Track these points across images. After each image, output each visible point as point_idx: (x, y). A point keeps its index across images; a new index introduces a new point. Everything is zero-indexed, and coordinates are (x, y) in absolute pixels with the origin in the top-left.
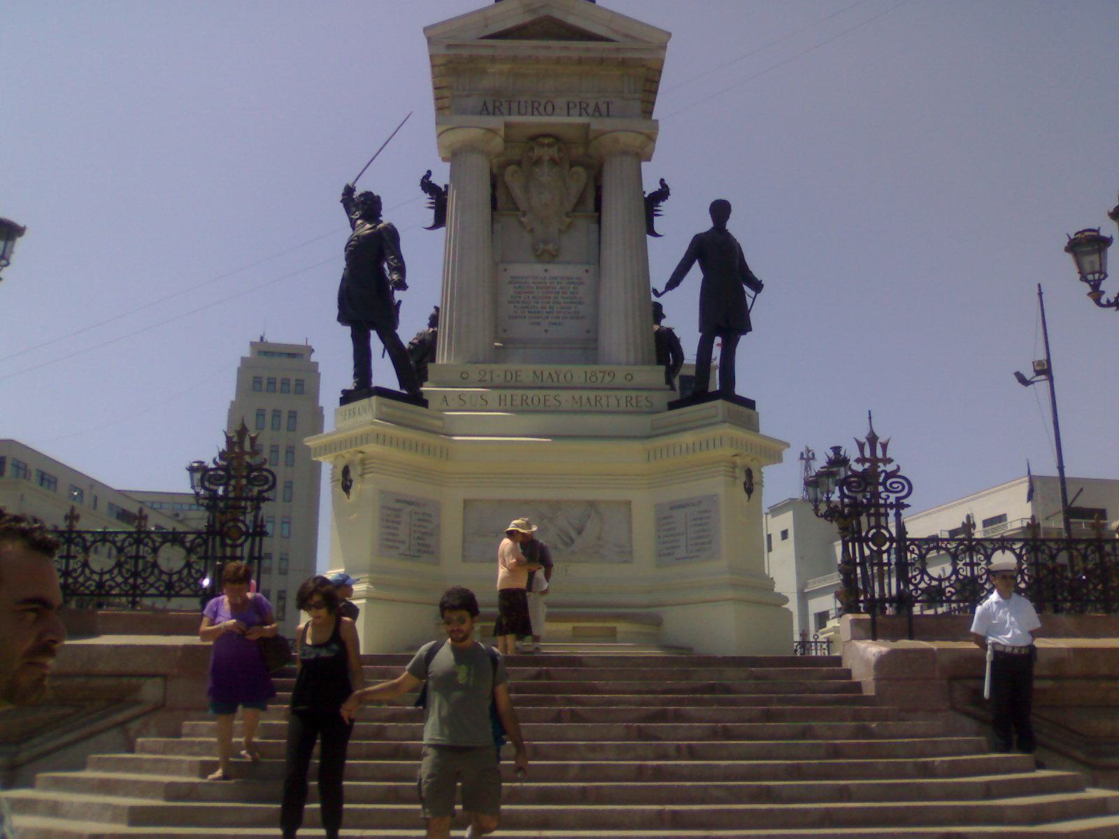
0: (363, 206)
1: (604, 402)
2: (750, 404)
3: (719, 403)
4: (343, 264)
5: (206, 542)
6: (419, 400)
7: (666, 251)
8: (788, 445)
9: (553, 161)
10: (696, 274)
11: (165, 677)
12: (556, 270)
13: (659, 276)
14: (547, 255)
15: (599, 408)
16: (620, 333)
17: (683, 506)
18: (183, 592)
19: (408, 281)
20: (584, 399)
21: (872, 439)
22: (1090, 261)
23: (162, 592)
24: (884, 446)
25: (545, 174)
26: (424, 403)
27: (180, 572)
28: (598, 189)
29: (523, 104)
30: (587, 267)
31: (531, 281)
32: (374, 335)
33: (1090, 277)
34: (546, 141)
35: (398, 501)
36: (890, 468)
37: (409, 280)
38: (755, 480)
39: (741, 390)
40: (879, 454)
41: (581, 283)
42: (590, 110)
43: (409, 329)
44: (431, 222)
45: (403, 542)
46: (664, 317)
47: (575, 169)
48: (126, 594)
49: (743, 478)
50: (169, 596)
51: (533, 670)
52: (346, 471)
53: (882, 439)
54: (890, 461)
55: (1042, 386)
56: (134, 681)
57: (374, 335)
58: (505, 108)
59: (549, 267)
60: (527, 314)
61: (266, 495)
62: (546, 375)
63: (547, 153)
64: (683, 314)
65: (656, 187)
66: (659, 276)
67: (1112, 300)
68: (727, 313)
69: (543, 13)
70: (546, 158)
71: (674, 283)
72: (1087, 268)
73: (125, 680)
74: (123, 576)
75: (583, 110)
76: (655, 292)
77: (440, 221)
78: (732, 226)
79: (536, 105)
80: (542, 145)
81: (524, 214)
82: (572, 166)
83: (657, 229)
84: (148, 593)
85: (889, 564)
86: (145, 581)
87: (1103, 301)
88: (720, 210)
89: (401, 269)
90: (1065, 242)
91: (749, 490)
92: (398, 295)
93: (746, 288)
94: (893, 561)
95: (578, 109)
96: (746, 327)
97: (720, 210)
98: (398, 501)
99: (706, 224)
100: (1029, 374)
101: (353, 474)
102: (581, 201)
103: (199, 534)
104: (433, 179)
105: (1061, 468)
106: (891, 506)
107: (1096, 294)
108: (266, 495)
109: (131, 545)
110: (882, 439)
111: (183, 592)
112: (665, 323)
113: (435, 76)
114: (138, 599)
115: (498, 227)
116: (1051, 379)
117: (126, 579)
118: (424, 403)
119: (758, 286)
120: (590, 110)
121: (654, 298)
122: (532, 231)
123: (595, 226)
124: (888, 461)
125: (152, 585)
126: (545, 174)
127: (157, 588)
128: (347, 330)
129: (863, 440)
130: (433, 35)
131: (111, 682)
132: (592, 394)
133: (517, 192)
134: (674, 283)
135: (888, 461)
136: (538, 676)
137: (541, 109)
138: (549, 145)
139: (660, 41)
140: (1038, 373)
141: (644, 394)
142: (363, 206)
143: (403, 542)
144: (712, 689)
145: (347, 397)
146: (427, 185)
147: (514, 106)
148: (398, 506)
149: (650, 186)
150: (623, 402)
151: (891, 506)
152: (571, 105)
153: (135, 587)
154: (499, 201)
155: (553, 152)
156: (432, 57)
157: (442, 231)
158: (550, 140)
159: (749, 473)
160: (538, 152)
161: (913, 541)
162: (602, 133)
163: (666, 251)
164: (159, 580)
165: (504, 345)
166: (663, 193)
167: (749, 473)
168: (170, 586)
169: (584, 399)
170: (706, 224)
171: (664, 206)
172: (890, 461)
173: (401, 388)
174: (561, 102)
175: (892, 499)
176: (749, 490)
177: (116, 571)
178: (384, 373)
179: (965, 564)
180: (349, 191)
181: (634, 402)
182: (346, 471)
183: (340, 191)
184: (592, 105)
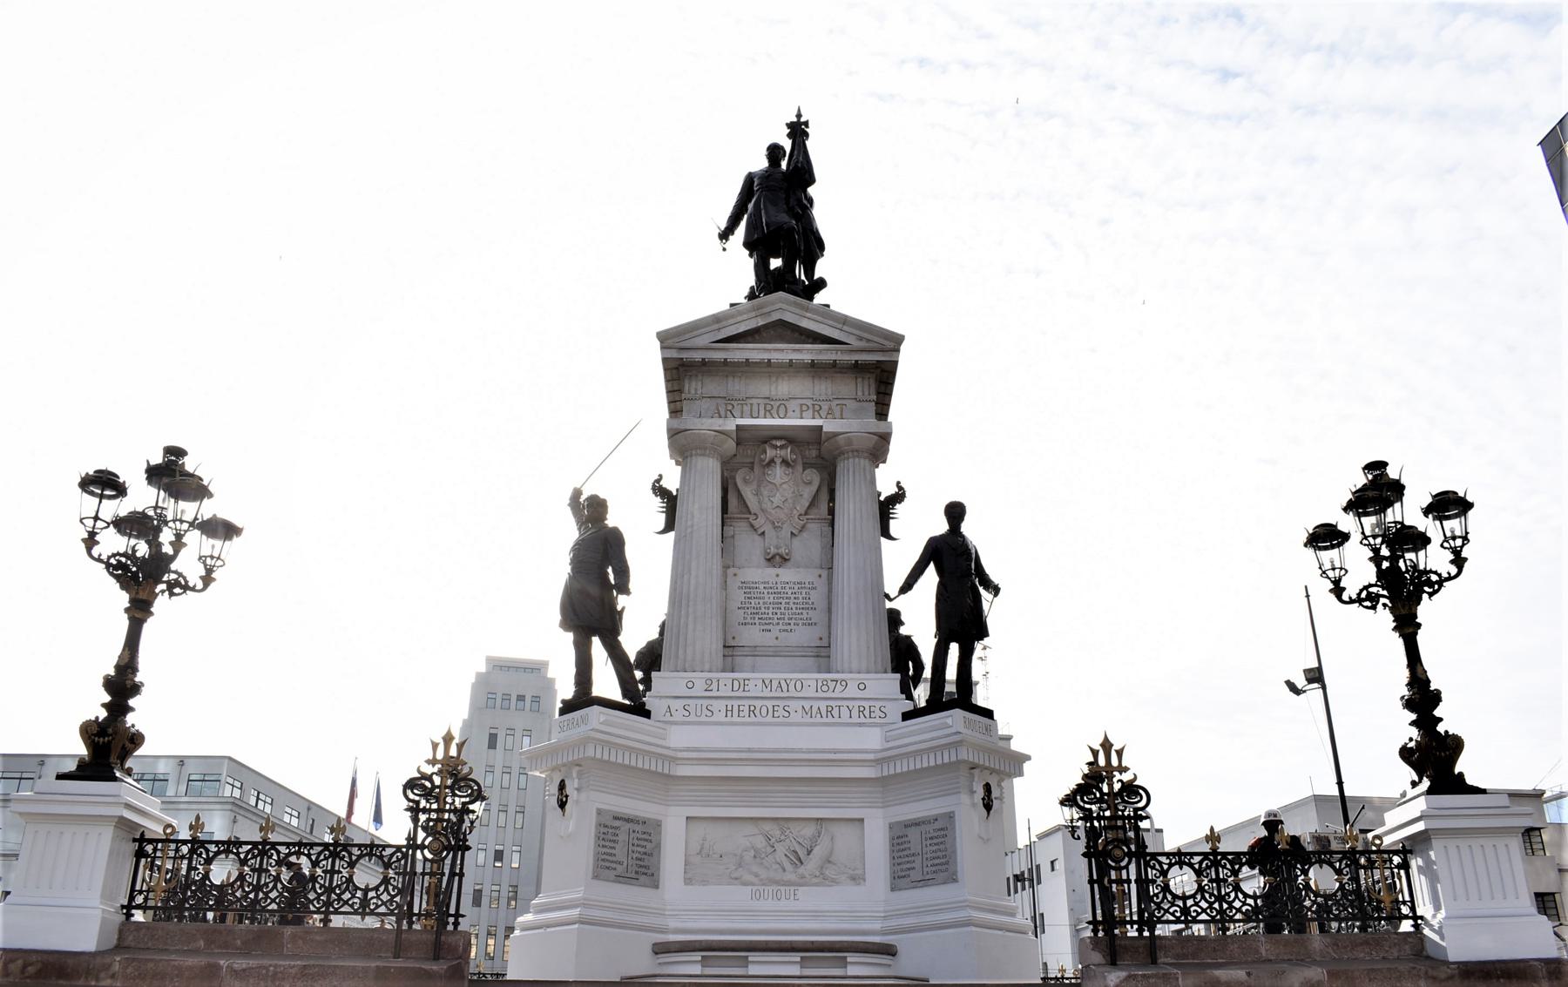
0: (591, 511)
1: (836, 712)
2: (988, 714)
3: (958, 713)
4: (568, 569)
6: (641, 710)
7: (900, 553)
8: (1028, 758)
9: (785, 462)
10: (931, 577)
12: (787, 574)
13: (893, 579)
14: (777, 560)
15: (830, 720)
16: (858, 640)
17: (917, 824)
19: (631, 586)
20: (815, 710)
21: (1107, 745)
22: (1328, 556)
24: (1120, 753)
25: (778, 474)
26: (647, 714)
27: (376, 889)
28: (832, 492)
29: (755, 408)
30: (820, 571)
32: (596, 641)
33: (1331, 574)
35: (616, 818)
36: (1126, 777)
37: (633, 585)
38: (993, 795)
39: (981, 698)
40: (1115, 762)
42: (823, 413)
43: (633, 640)
44: (662, 526)
46: (902, 623)
49: (980, 793)
50: (363, 915)
53: (1116, 747)
54: (1126, 769)
55: (1315, 693)
57: (596, 641)
59: (779, 571)
61: (471, 807)
62: (775, 684)
64: (920, 619)
65: (894, 490)
66: (893, 579)
67: (1354, 597)
68: (963, 620)
69: (775, 317)
71: (907, 587)
72: (1327, 566)
75: (817, 412)
76: (887, 596)
77: (669, 526)
78: (966, 528)
80: (776, 447)
83: (893, 532)
85: (1128, 881)
87: (1345, 597)
88: (955, 513)
89: (623, 572)
90: (1304, 537)
91: (988, 807)
92: (622, 601)
93: (981, 589)
94: (1133, 877)
96: (982, 632)
97: (955, 513)
98: (616, 818)
99: (941, 527)
100: (1300, 682)
101: (569, 790)
102: (812, 504)
103: (399, 848)
104: (664, 483)
105: (1340, 783)
107: (1338, 590)
108: (471, 807)
110: (1116, 747)
112: (903, 631)
113: (667, 381)
115: (729, 531)
116: (1324, 688)
118: (647, 714)
119: (996, 590)
120: (823, 413)
121: (889, 605)
123: (828, 529)
124: (1123, 769)
126: (778, 474)
128: (570, 636)
129: (1097, 747)
130: (667, 339)
132: (823, 705)
133: (748, 493)
134: (907, 587)
135: (1123, 769)
138: (782, 447)
139: (893, 342)
140: (1310, 681)
141: (878, 704)
142: (591, 511)
145: (568, 707)
146: (659, 490)
148: (617, 823)
149: (886, 489)
150: (855, 713)
154: (730, 505)
155: (787, 453)
156: (665, 360)
157: (672, 535)
159: (988, 788)
161: (1154, 856)
162: (836, 435)
163: (900, 553)
165: (731, 653)
166: (899, 497)
167: (988, 788)
168: (365, 902)
169: (815, 710)
170: (941, 527)
172: (1126, 769)
173: (624, 696)
174: (793, 405)
176: (988, 807)
178: (606, 683)
179: (1211, 881)
180: (577, 494)
181: (867, 713)
182: (562, 786)
183: (569, 494)
184: (825, 407)
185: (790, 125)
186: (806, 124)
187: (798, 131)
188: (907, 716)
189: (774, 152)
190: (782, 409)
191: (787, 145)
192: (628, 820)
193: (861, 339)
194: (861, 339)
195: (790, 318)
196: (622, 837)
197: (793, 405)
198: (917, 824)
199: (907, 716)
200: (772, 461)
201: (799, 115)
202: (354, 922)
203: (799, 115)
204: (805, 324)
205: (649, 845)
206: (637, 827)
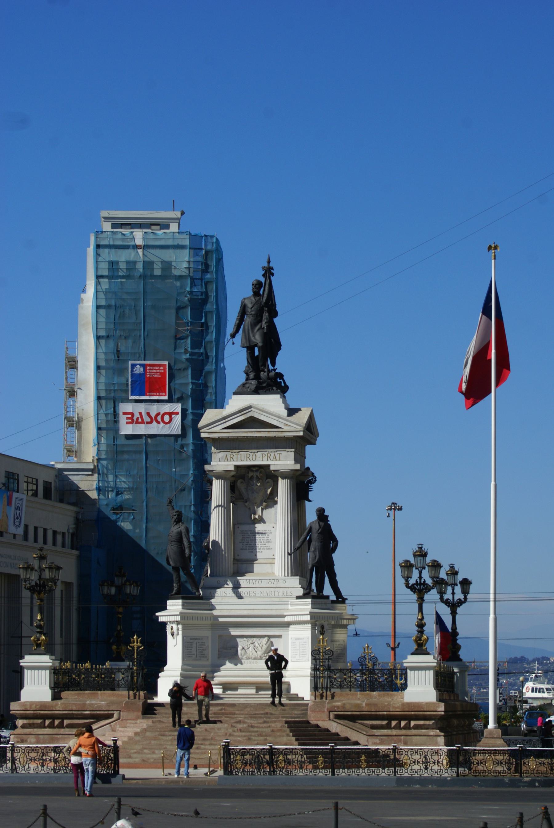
5: (127, 671)
11: (120, 711)
17: (299, 639)
31: (249, 532)
34: (254, 469)
35: (191, 639)
41: (271, 533)
45: (194, 654)
47: (268, 480)
51: (220, 708)
52: (172, 629)
56: (112, 712)
58: (235, 459)
60: (247, 548)
63: (255, 474)
70: (255, 476)
73: (110, 712)
79: (248, 456)
80: (253, 471)
81: (246, 502)
82: (267, 479)
95: (266, 457)
103: (125, 669)
106: (327, 659)
120: (272, 458)
122: (250, 508)
131: (106, 712)
133: (243, 490)
136: (221, 710)
137: (251, 458)
138: (256, 471)
143: (194, 654)
144: (267, 713)
147: (239, 456)
148: (192, 641)
151: (327, 659)
152: (264, 455)
155: (258, 474)
158: (257, 468)
159: (322, 627)
160: (251, 474)
171: (314, 486)
175: (327, 657)
182: (172, 629)
185: (263, 268)
186: (273, 269)
187: (268, 272)
188: (298, 598)
189: (258, 286)
190: (254, 455)
191: (263, 280)
192: (196, 639)
193: (286, 425)
194: (286, 425)
195: (256, 416)
196: (194, 645)
197: (259, 454)
198: (299, 639)
199: (298, 598)
200: (252, 477)
201: (269, 262)
203: (269, 262)
204: (262, 418)
205: (204, 646)
206: (199, 641)
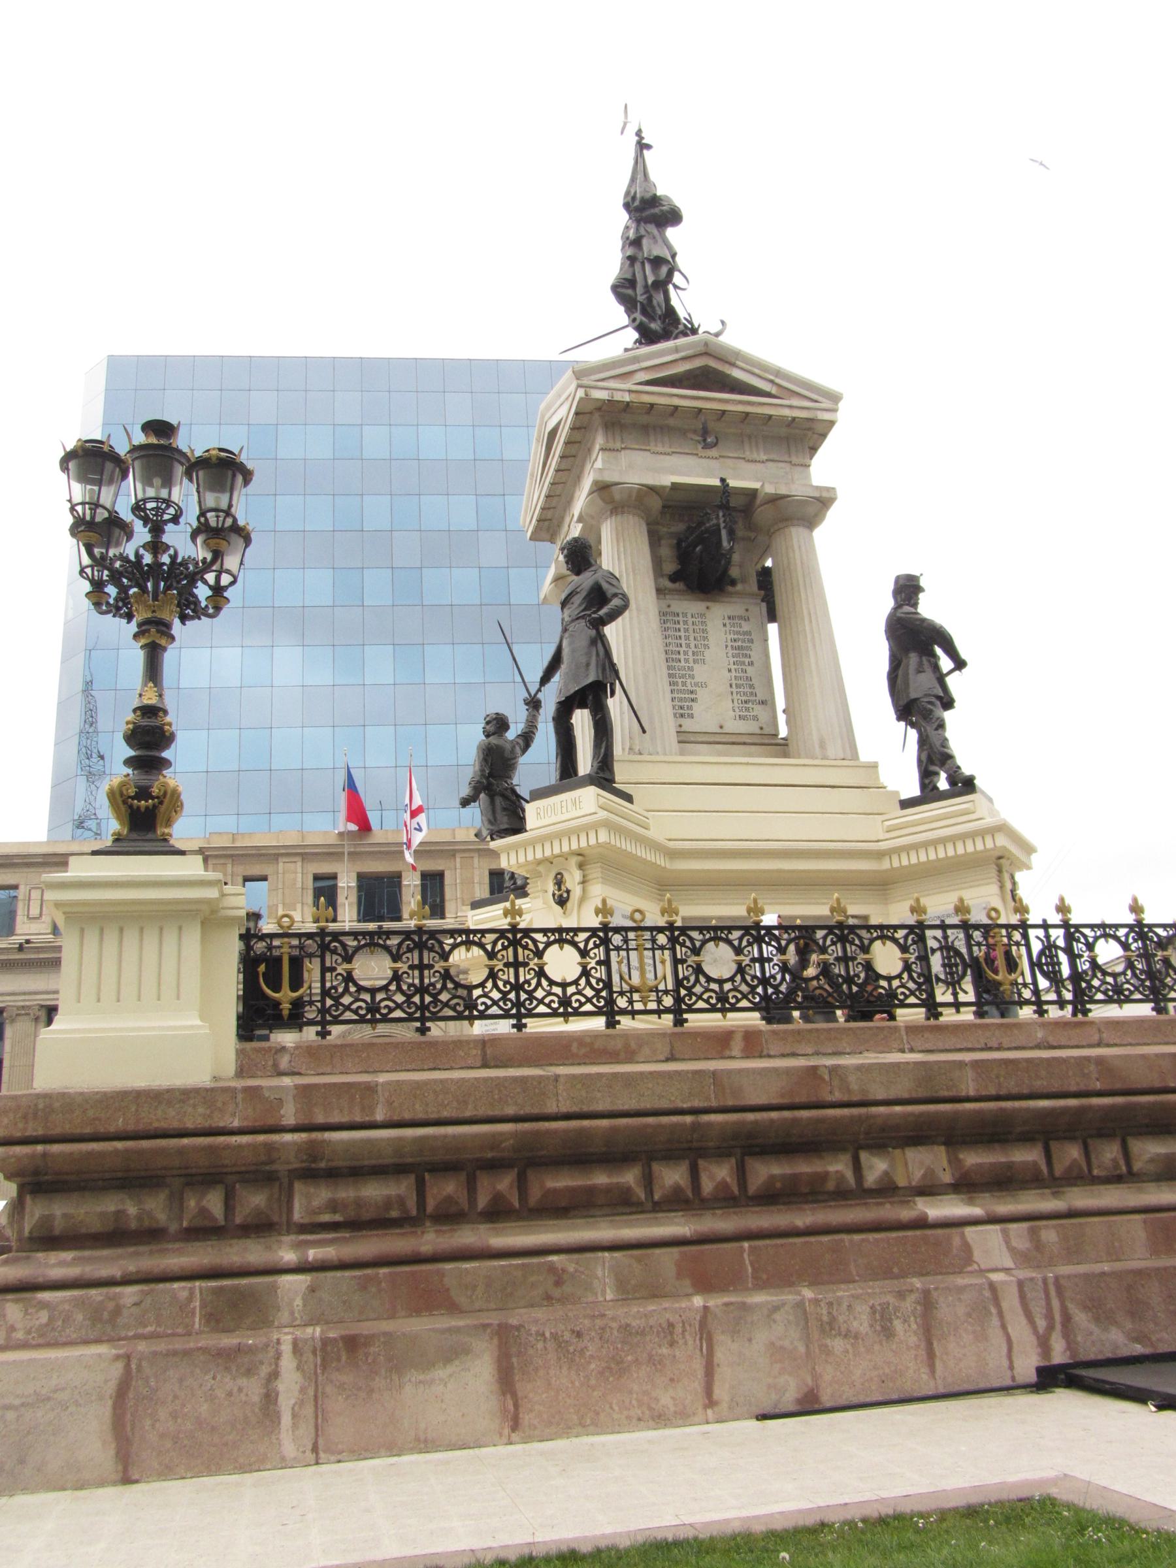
18: (583, 1009)
23: (555, 1010)
48: (506, 1015)
50: (471, 1019)
74: (499, 990)
84: (695, 1007)
86: (531, 997)
109: (505, 948)
111: (583, 1009)
114: (428, 1024)
117: (505, 994)
125: (541, 1002)
127: (548, 1006)
153: (518, 1004)
164: (549, 994)
168: (565, 1001)
177: (489, 985)
202: (556, 1026)
